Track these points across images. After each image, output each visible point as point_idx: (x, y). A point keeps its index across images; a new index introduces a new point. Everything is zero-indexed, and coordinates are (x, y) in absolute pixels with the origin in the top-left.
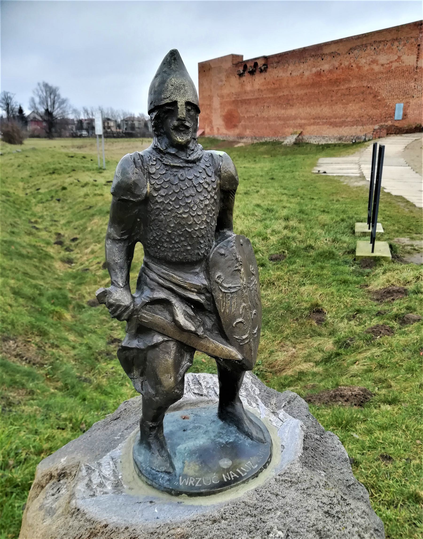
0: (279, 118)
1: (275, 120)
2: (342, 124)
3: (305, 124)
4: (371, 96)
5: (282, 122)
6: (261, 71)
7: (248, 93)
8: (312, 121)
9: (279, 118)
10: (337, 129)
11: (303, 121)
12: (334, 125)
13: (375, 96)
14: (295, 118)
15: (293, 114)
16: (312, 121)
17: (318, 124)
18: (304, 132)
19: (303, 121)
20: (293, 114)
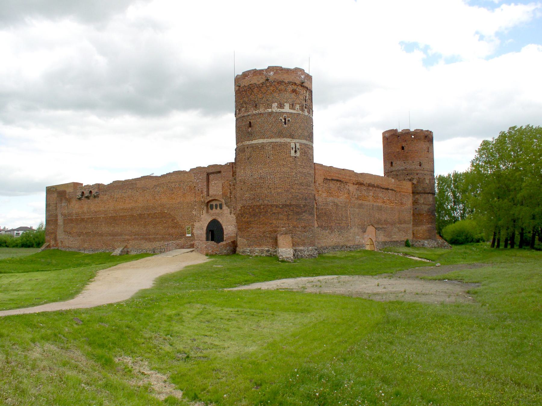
0: (110, 235)
1: (106, 236)
2: (154, 240)
3: (128, 240)
4: (170, 220)
5: (112, 238)
6: (95, 197)
7: (85, 213)
8: (133, 237)
9: (110, 235)
10: (151, 243)
11: (127, 237)
12: (150, 240)
13: (172, 220)
14: (121, 235)
15: (119, 231)
16: (133, 237)
17: (137, 239)
18: (129, 246)
19: (127, 237)
20: (119, 231)
